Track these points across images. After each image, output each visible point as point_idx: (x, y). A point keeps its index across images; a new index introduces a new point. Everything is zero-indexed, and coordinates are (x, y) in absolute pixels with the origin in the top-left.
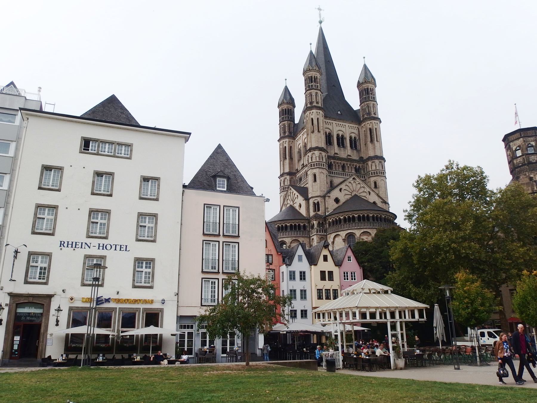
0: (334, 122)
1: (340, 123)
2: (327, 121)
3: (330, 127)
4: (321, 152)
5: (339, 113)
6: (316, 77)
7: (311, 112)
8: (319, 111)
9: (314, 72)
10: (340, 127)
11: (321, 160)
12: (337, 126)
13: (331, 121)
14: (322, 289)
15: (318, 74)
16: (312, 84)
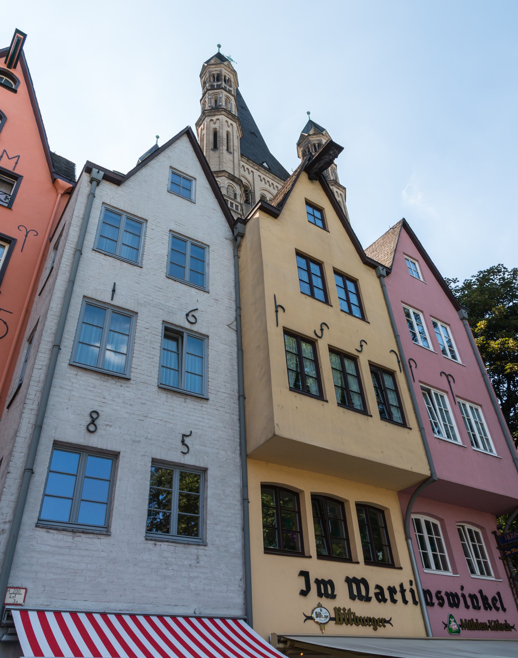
0: (256, 173)
1: (267, 179)
2: (242, 163)
3: (250, 177)
4: (231, 182)
5: (265, 164)
6: (227, 78)
7: (214, 118)
8: (230, 122)
9: (223, 69)
10: (267, 186)
11: (233, 197)
12: (261, 180)
13: (251, 169)
14: (312, 343)
15: (232, 76)
16: (219, 83)
